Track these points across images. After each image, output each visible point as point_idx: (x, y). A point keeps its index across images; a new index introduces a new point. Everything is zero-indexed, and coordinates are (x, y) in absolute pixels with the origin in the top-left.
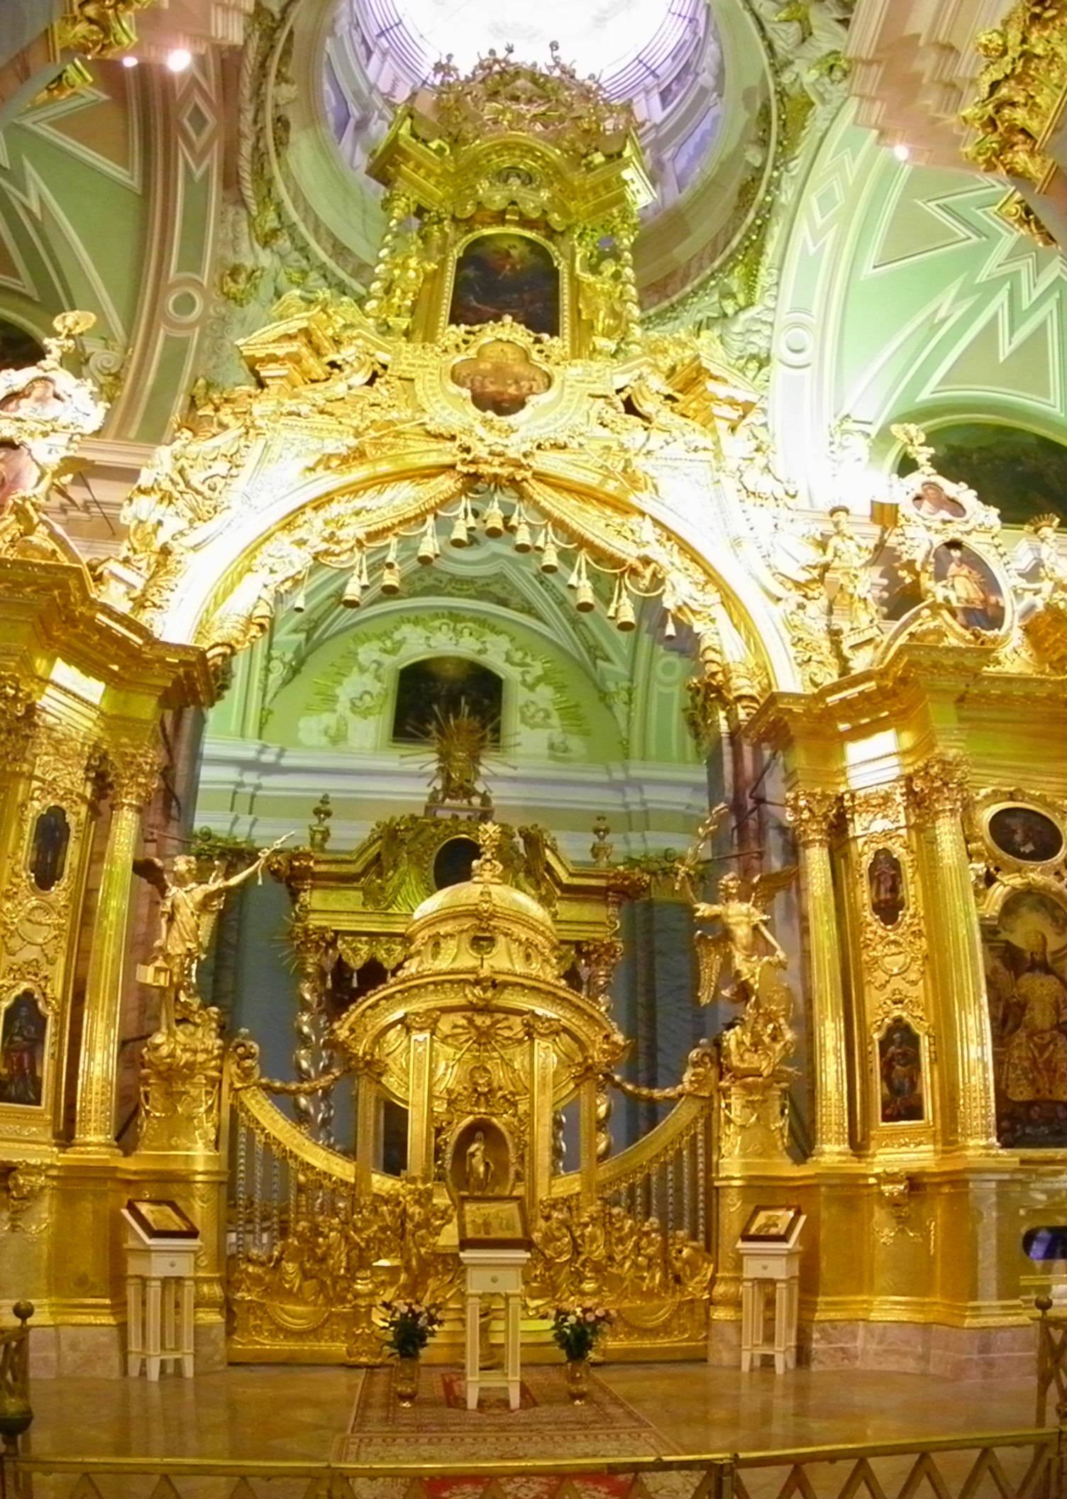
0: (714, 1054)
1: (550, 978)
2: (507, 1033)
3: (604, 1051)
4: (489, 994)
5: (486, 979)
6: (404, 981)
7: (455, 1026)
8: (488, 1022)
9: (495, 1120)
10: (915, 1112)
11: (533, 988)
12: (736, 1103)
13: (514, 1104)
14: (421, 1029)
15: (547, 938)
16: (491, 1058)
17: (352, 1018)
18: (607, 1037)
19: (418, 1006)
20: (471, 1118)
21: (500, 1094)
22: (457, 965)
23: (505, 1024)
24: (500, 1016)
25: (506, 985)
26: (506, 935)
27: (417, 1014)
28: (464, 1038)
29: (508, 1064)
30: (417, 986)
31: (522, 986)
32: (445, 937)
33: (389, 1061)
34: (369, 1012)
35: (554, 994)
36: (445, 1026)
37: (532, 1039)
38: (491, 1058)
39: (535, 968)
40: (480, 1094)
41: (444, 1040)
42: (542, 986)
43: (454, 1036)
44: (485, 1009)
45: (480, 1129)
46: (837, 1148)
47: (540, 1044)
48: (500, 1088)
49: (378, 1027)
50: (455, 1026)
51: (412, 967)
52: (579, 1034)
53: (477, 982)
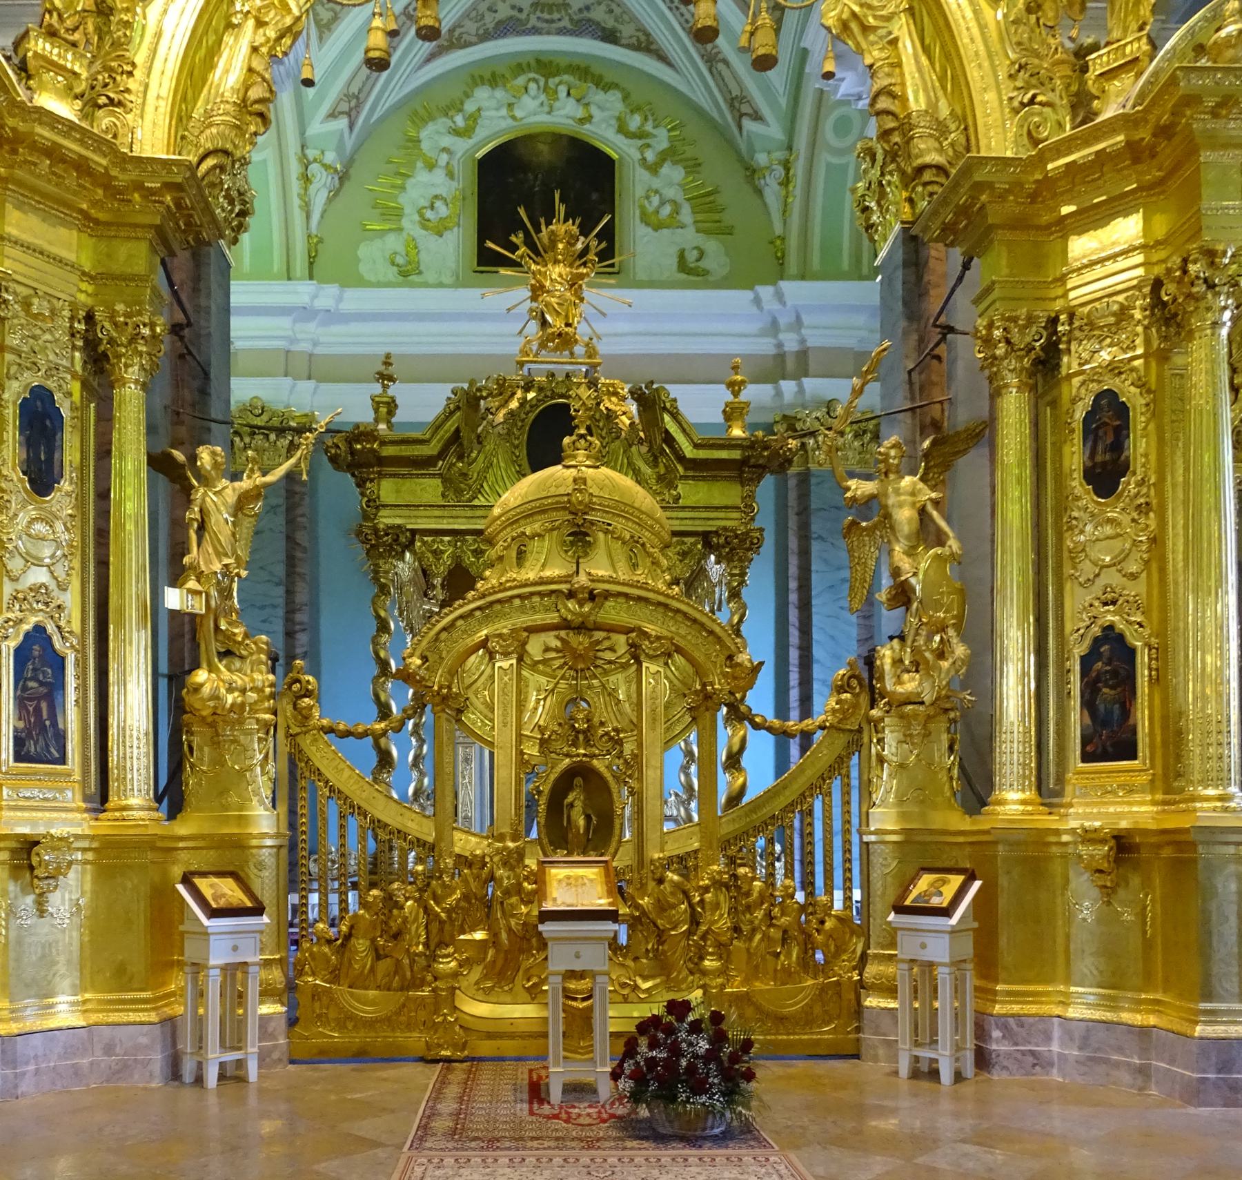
0: (865, 675)
1: (661, 586)
2: (609, 655)
3: (725, 675)
4: (586, 609)
5: (583, 588)
6: (484, 596)
7: (547, 649)
8: (586, 642)
9: (595, 762)
10: (1127, 750)
11: (640, 599)
12: (890, 737)
13: (620, 742)
14: (506, 655)
15: (656, 534)
16: (590, 687)
17: (424, 643)
18: (730, 658)
19: (504, 626)
20: (567, 761)
21: (600, 732)
22: (548, 573)
23: (606, 644)
24: (599, 635)
25: (607, 595)
26: (606, 532)
27: (500, 636)
28: (557, 664)
29: (612, 694)
30: (499, 601)
31: (626, 595)
32: (532, 537)
33: (470, 695)
34: (444, 635)
35: (666, 606)
36: (535, 648)
37: (639, 663)
38: (590, 687)
39: (640, 576)
40: (578, 732)
41: (534, 666)
42: (650, 595)
43: (545, 662)
44: (582, 627)
45: (580, 774)
46: (1020, 796)
47: (649, 667)
48: (602, 724)
49: (454, 653)
50: (547, 649)
51: (492, 579)
52: (696, 654)
53: (571, 595)
